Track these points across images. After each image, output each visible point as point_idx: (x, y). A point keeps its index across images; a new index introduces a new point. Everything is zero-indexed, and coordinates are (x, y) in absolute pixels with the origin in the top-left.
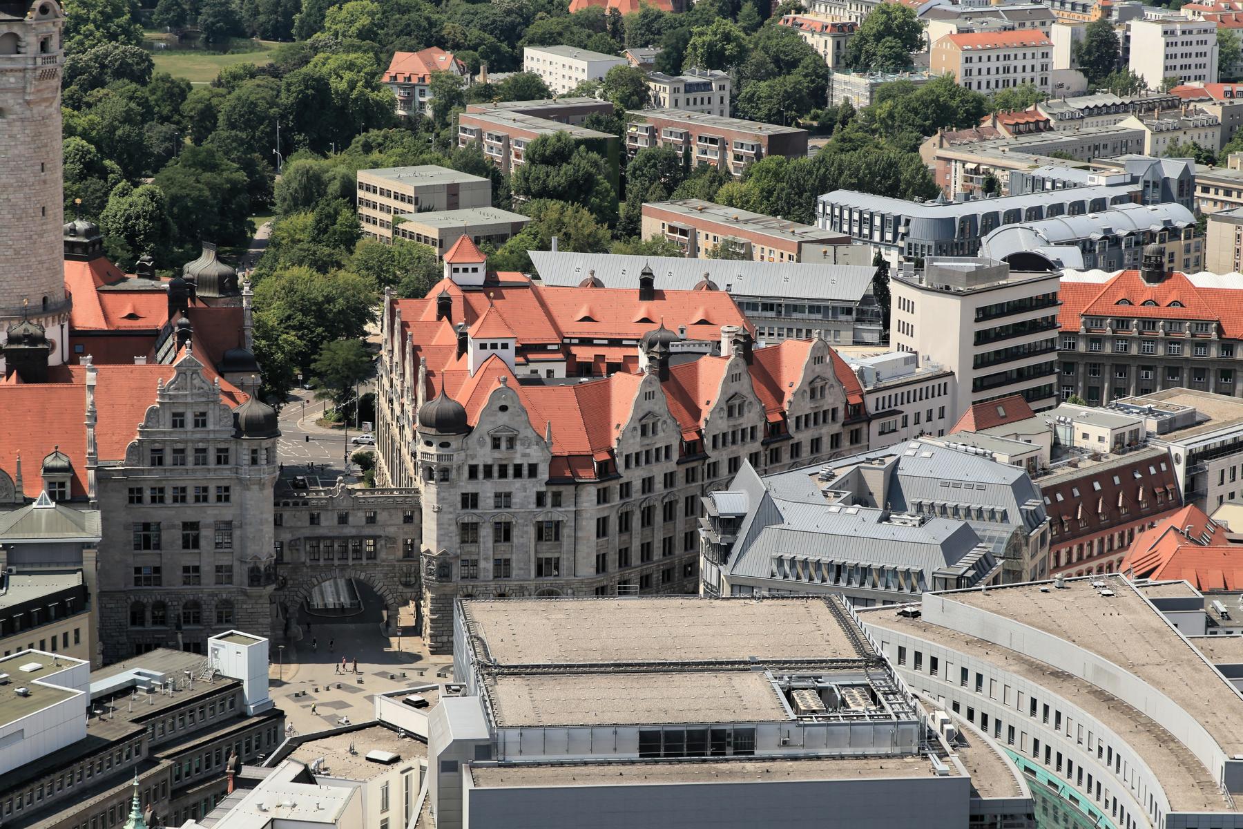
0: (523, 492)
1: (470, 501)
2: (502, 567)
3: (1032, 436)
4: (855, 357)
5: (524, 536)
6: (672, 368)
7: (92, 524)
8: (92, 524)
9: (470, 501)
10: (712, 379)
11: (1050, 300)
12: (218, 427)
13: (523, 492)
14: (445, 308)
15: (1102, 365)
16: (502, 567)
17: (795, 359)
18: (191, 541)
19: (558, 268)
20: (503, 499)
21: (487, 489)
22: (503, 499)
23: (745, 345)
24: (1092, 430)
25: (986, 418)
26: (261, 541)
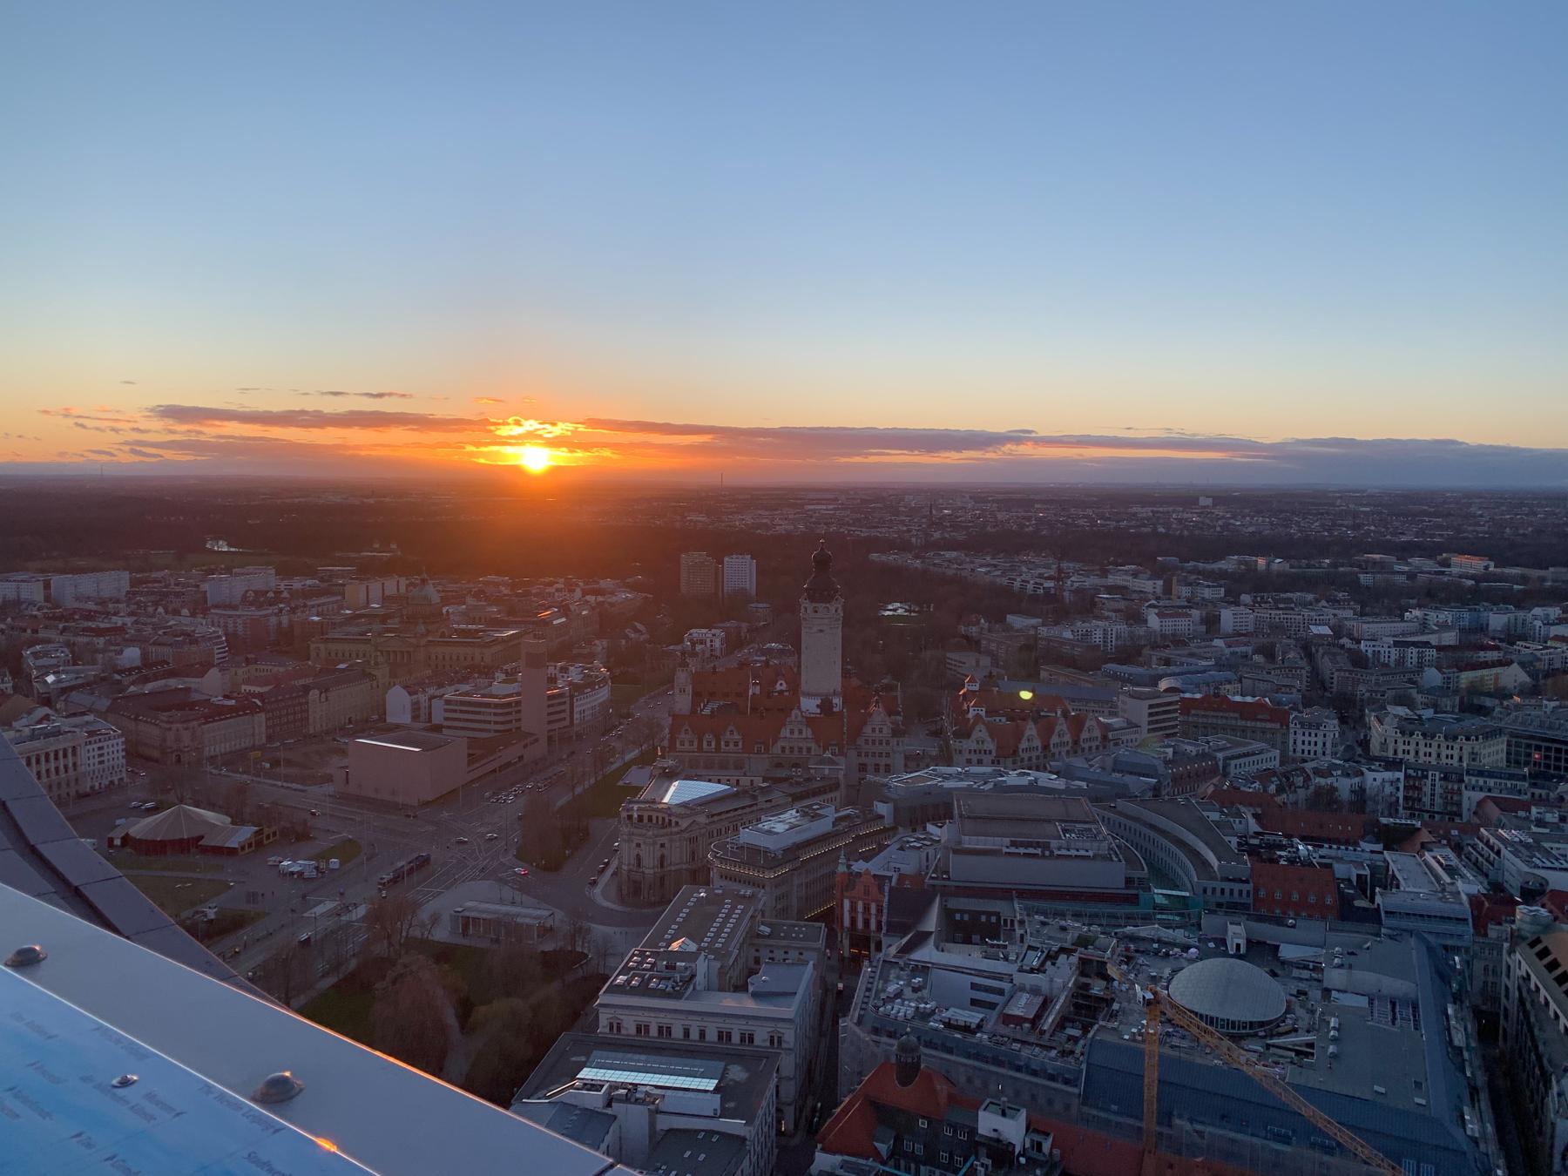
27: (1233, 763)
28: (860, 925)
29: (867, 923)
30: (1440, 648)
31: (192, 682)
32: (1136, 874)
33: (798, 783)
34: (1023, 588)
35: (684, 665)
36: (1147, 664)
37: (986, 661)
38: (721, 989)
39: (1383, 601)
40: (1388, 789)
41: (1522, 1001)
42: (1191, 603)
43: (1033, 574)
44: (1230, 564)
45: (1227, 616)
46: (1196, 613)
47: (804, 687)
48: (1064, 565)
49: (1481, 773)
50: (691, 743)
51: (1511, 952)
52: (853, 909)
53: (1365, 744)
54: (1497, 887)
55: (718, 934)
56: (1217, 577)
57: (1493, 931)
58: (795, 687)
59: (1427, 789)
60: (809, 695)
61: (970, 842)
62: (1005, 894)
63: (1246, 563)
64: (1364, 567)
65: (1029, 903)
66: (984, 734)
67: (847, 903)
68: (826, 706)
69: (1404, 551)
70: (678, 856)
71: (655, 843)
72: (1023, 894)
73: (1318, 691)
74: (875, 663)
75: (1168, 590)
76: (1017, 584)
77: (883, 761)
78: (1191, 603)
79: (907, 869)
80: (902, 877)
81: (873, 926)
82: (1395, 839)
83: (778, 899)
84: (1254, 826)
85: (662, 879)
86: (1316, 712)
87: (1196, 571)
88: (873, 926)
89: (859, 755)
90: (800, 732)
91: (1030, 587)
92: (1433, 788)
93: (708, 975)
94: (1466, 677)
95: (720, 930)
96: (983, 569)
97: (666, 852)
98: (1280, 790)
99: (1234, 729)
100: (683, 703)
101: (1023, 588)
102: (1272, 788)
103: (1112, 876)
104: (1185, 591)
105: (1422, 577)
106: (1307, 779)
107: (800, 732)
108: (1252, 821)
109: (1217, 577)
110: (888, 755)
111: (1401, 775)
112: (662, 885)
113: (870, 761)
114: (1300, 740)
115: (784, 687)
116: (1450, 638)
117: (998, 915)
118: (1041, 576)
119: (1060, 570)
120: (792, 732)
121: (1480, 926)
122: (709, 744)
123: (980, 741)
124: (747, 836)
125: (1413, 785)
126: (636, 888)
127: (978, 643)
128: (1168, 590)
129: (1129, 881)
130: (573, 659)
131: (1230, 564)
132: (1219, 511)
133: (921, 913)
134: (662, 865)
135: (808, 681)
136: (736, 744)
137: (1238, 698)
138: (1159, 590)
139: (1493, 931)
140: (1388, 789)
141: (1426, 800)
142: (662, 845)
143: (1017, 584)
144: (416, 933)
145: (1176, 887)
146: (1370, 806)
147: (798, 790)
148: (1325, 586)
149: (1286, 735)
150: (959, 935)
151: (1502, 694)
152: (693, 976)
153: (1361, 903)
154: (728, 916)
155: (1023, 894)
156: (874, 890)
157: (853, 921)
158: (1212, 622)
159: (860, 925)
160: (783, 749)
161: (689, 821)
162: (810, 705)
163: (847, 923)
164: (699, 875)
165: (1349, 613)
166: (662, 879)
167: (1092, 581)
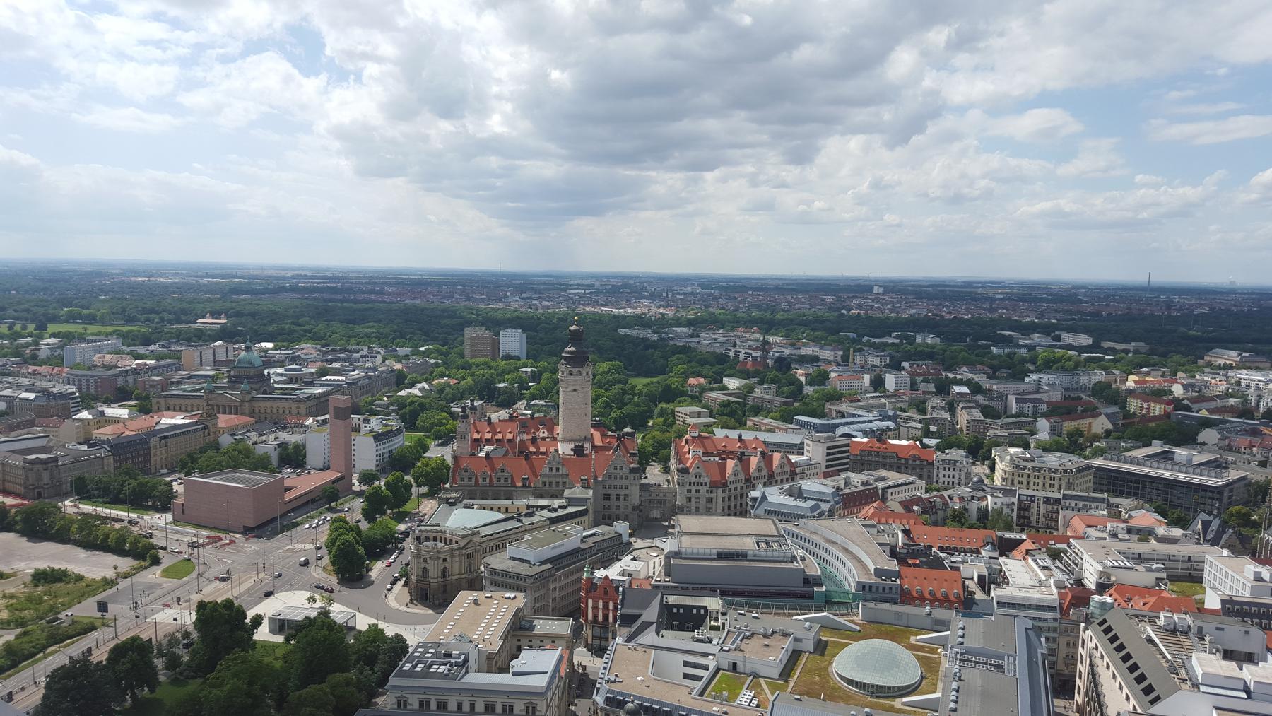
0: (703, 489)
1: (689, 491)
2: (697, 508)
3: (840, 480)
4: (794, 458)
5: (703, 501)
6: (743, 459)
7: (590, 493)
8: (590, 493)
9: (689, 491)
10: (754, 461)
11: (848, 445)
12: (626, 470)
13: (703, 489)
14: (687, 441)
15: (864, 461)
16: (697, 508)
17: (777, 457)
18: (618, 498)
19: (720, 433)
20: (697, 491)
21: (694, 488)
22: (697, 491)
23: (763, 454)
24: (857, 478)
25: (826, 475)
26: (635, 499)
27: (890, 491)
28: (601, 619)
29: (606, 617)
33: (556, 510)
41: (1091, 665)
50: (470, 479)
51: (1086, 629)
52: (595, 608)
55: (487, 628)
60: (566, 441)
67: (590, 602)
68: (579, 451)
71: (438, 558)
81: (611, 619)
83: (537, 600)
85: (445, 586)
88: (611, 619)
89: (604, 487)
90: (558, 470)
95: (488, 625)
97: (448, 566)
107: (558, 470)
110: (626, 488)
112: (445, 591)
113: (613, 492)
115: (546, 434)
120: (551, 470)
121: (1064, 612)
122: (484, 480)
130: (373, 413)
134: (444, 576)
136: (506, 479)
142: (445, 560)
147: (555, 514)
156: (612, 592)
157: (595, 616)
159: (601, 619)
160: (544, 483)
161: (466, 541)
162: (565, 449)
163: (590, 616)
166: (445, 586)
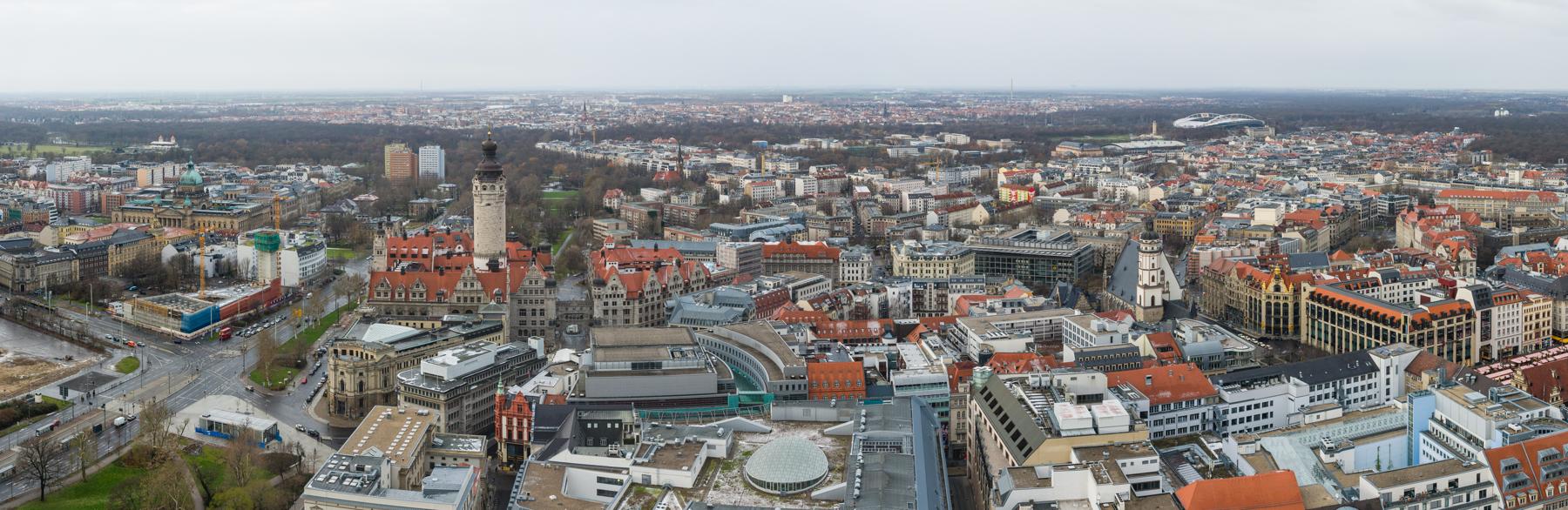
30: (937, 198)
31: (33, 235)
32: (725, 380)
34: (654, 168)
35: (382, 233)
36: (743, 222)
37: (623, 225)
38: (402, 488)
39: (910, 169)
40: (903, 299)
42: (775, 175)
43: (660, 157)
44: (802, 145)
45: (800, 186)
46: (778, 183)
47: (477, 250)
48: (686, 149)
49: (958, 281)
53: (890, 268)
54: (966, 357)
56: (791, 154)
57: (961, 388)
58: (469, 252)
59: (927, 296)
61: (600, 366)
62: (624, 404)
63: (814, 143)
64: (891, 145)
65: (645, 411)
66: (617, 283)
69: (918, 131)
70: (373, 382)
72: (640, 404)
73: (859, 236)
74: (533, 231)
75: (759, 166)
76: (649, 165)
77: (538, 307)
78: (775, 175)
79: (554, 391)
80: (548, 396)
82: (902, 333)
84: (810, 336)
86: (857, 250)
87: (779, 151)
91: (659, 166)
92: (931, 295)
93: (390, 476)
94: (953, 216)
96: (624, 155)
98: (831, 309)
99: (801, 265)
100: (380, 263)
101: (654, 168)
102: (826, 307)
103: (706, 384)
104: (769, 166)
105: (927, 150)
106: (850, 298)
108: (809, 332)
109: (791, 154)
111: (910, 288)
114: (847, 272)
116: (943, 191)
117: (620, 422)
118: (667, 158)
119: (681, 153)
123: (615, 288)
124: (426, 367)
125: (918, 296)
126: (340, 406)
127: (618, 212)
128: (759, 166)
129: (721, 387)
131: (802, 145)
132: (796, 106)
133: (560, 419)
135: (479, 244)
137: (805, 243)
138: (753, 166)
139: (961, 388)
140: (903, 299)
141: (927, 303)
143: (649, 165)
144: (172, 430)
145: (755, 389)
146: (891, 313)
148: (875, 159)
149: (837, 269)
150: (590, 440)
151: (973, 227)
152: (378, 476)
153: (881, 383)
154: (409, 430)
155: (640, 404)
158: (789, 188)
164: (389, 399)
165: (881, 177)
167: (704, 160)
